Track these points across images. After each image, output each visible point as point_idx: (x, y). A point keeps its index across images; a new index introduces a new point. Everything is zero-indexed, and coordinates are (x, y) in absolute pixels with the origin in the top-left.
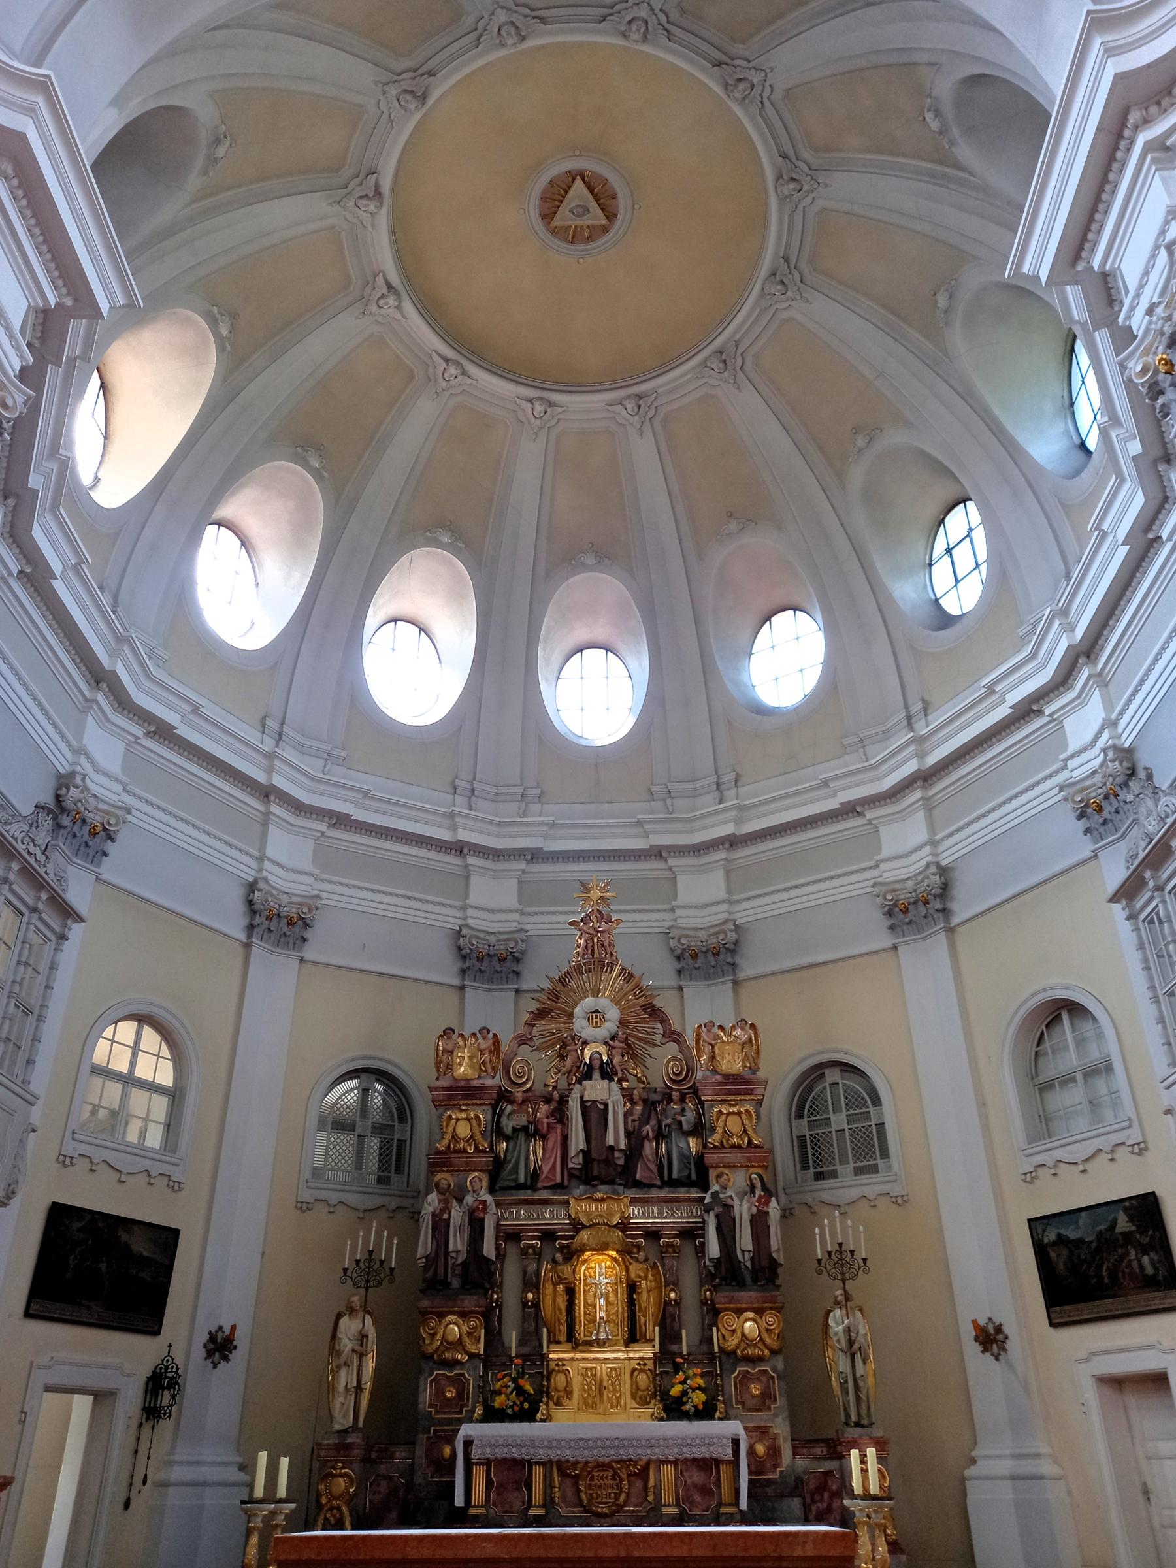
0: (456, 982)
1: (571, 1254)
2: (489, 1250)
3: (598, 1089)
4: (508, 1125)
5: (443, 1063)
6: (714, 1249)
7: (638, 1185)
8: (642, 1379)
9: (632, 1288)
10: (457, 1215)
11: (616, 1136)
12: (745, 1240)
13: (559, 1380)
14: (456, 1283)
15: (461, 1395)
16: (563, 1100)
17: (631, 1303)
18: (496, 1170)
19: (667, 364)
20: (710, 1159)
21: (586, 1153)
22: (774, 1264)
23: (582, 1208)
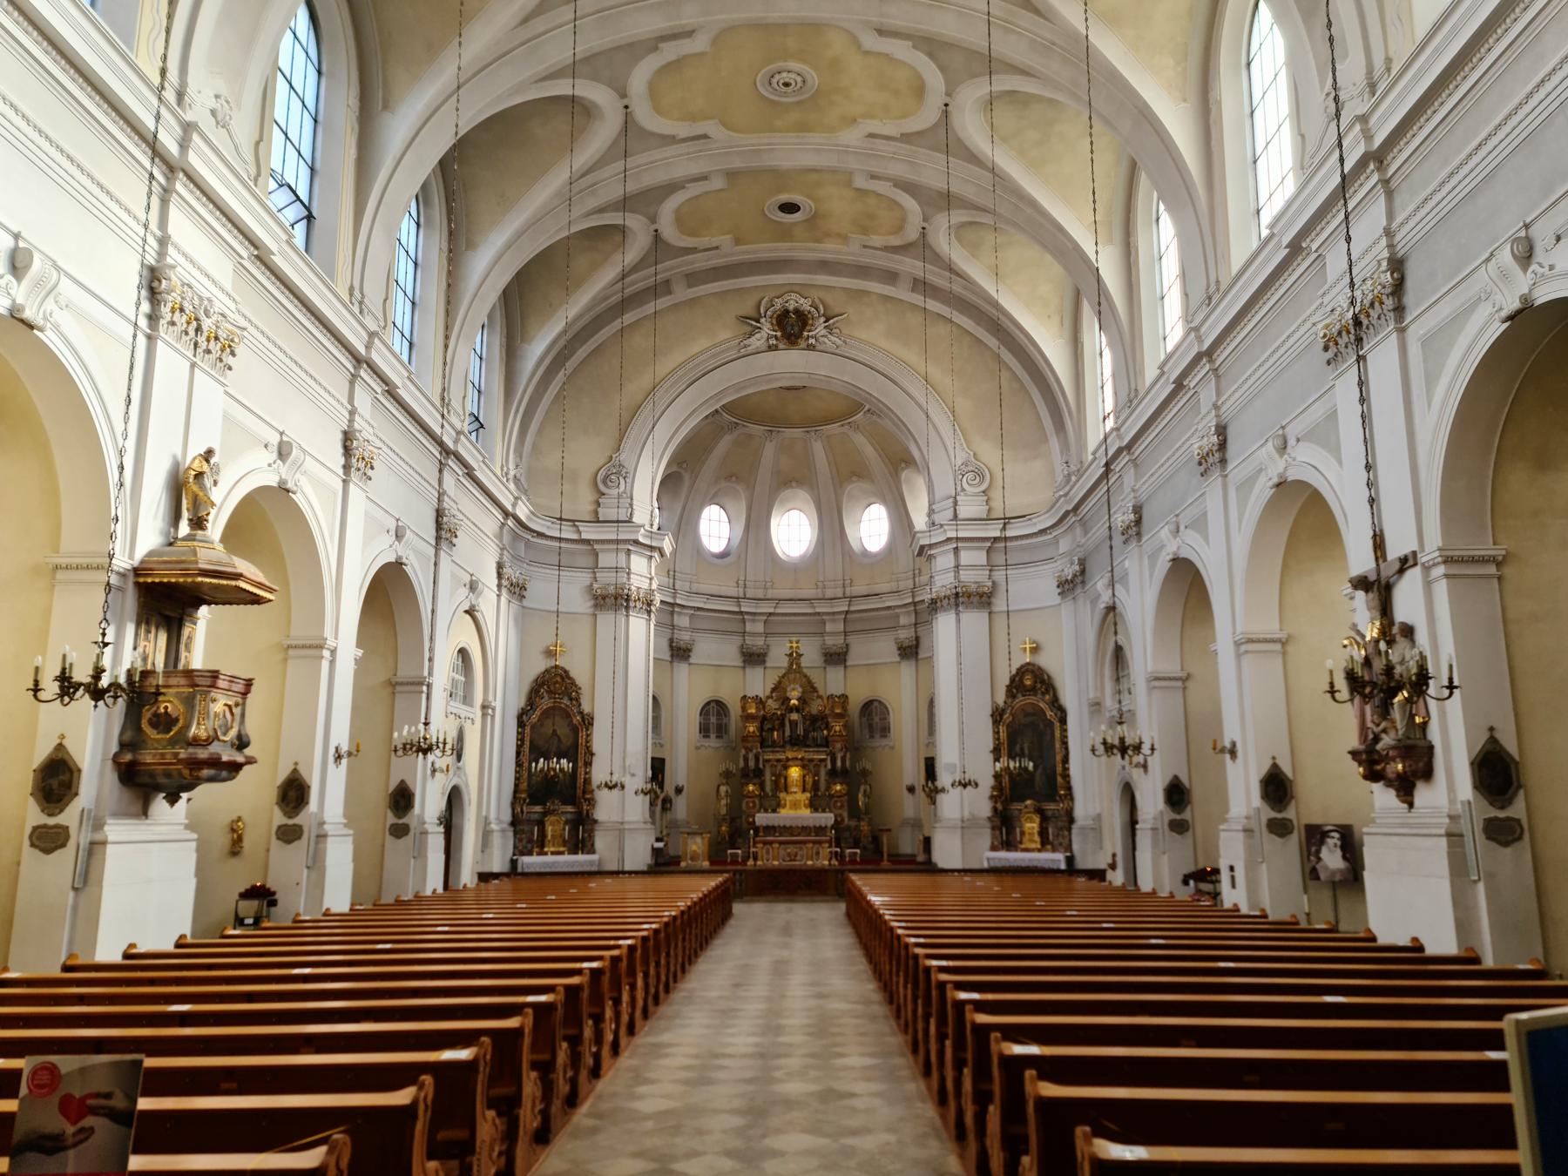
0: (742, 665)
1: (786, 768)
2: (761, 766)
3: (794, 716)
4: (766, 728)
5: (744, 708)
6: (829, 766)
7: (809, 746)
8: (807, 802)
9: (804, 776)
10: (751, 756)
11: (800, 731)
12: (839, 763)
13: (783, 802)
14: (751, 775)
15: (754, 806)
16: (783, 720)
17: (804, 781)
18: (763, 744)
19: (828, 421)
20: (830, 739)
21: (790, 736)
22: (847, 771)
23: (790, 755)
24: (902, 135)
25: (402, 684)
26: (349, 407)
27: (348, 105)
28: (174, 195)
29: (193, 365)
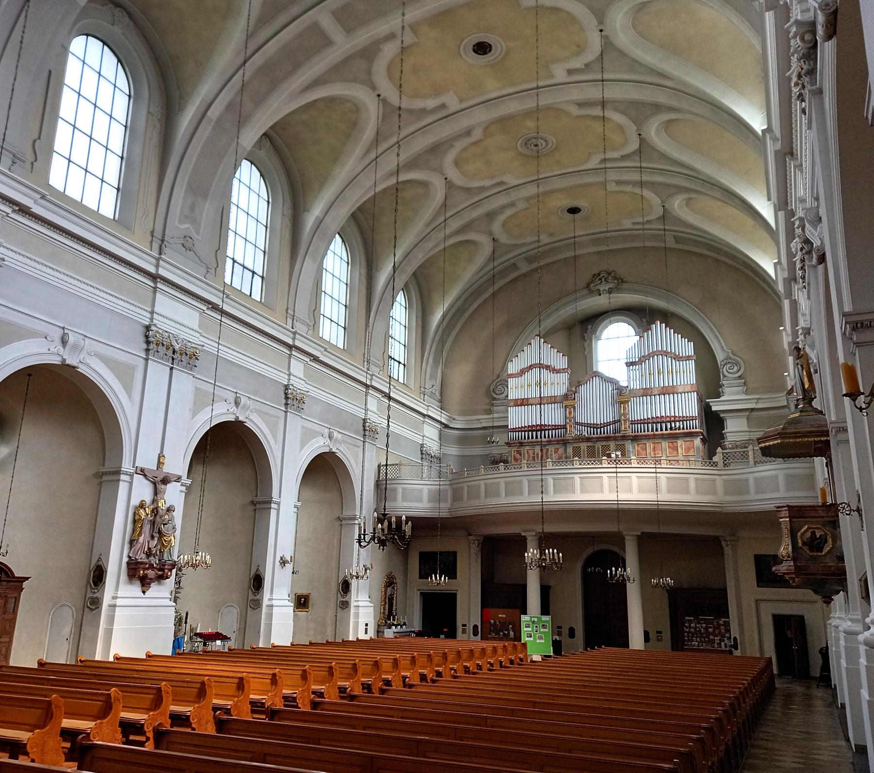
24: (621, 156)
25: (345, 519)
26: (288, 373)
27: (283, 214)
28: (158, 289)
29: (172, 369)
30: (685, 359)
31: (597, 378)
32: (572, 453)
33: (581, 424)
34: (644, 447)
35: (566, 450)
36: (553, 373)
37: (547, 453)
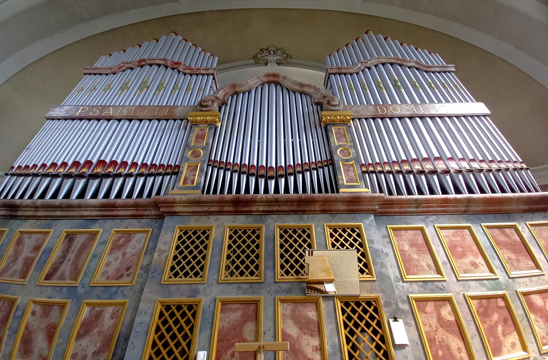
30: (438, 69)
31: (273, 86)
32: (173, 252)
33: (225, 166)
34: (420, 239)
35: (155, 238)
36: (185, 74)
37: (84, 247)
